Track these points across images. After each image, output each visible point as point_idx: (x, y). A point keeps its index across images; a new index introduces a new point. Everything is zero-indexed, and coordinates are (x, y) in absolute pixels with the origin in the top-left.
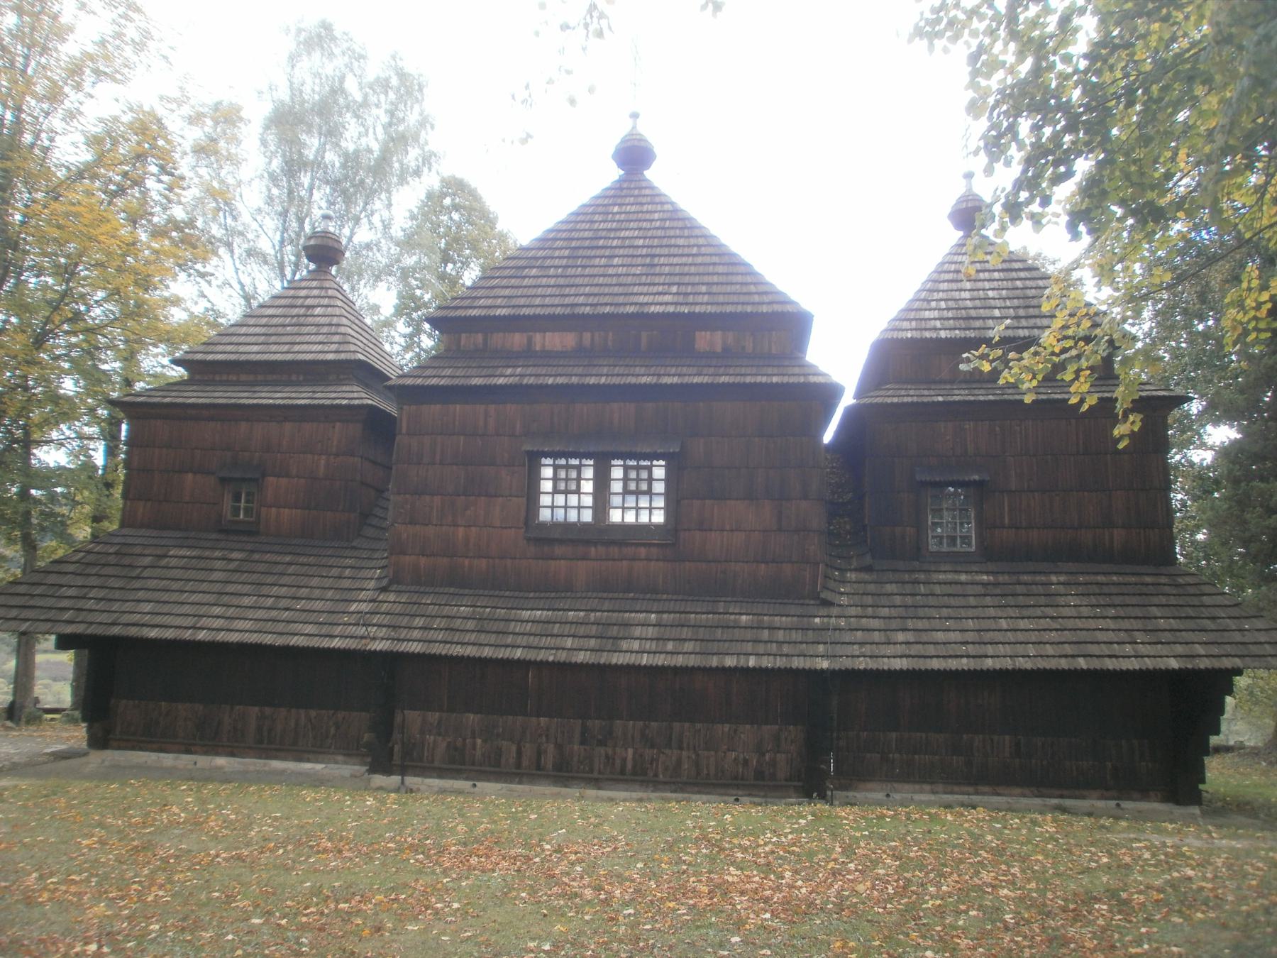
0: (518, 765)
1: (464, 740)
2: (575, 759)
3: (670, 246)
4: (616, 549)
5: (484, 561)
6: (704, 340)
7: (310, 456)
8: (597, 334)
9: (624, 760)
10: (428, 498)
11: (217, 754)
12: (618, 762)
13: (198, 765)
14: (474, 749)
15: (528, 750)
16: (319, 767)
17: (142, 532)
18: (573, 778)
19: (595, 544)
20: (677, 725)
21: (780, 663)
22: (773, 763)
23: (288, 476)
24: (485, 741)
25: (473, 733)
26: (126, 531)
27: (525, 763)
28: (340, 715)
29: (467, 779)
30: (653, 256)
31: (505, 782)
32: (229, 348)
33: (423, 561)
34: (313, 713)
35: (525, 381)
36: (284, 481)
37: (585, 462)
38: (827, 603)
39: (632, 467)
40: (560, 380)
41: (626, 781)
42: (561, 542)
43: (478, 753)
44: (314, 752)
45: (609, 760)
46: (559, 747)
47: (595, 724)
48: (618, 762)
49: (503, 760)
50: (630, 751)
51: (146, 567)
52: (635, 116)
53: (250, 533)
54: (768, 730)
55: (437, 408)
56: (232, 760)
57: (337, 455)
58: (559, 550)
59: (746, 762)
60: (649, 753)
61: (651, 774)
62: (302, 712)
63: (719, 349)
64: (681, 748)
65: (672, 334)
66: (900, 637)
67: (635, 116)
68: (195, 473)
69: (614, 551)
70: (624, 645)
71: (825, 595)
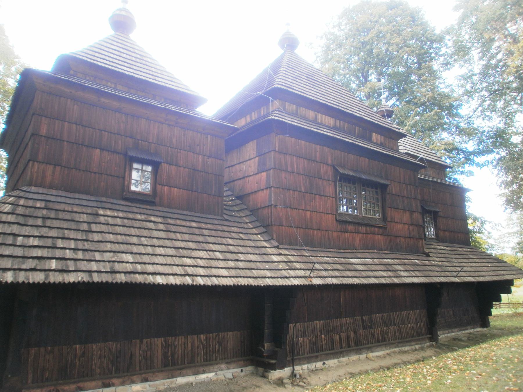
16: (211, 375)
17: (54, 192)
23: (177, 165)
24: (325, 336)
25: (321, 332)
28: (221, 335)
29: (321, 360)
31: (338, 358)
34: (203, 337)
44: (206, 365)
46: (355, 332)
47: (366, 317)
53: (152, 203)
56: (146, 385)
57: (209, 157)
58: (350, 227)
60: (386, 328)
68: (102, 149)
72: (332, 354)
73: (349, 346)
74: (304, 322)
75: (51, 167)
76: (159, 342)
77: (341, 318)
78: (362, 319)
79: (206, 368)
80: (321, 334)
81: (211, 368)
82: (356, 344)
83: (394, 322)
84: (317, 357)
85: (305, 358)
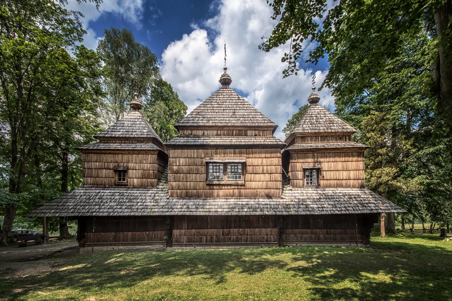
5: (195, 191)
6: (249, 133)
10: (179, 175)
37: (221, 164)
39: (233, 166)
52: (225, 69)
64: (247, 235)
67: (225, 69)
71: (282, 196)
74: (185, 229)
77: (207, 229)
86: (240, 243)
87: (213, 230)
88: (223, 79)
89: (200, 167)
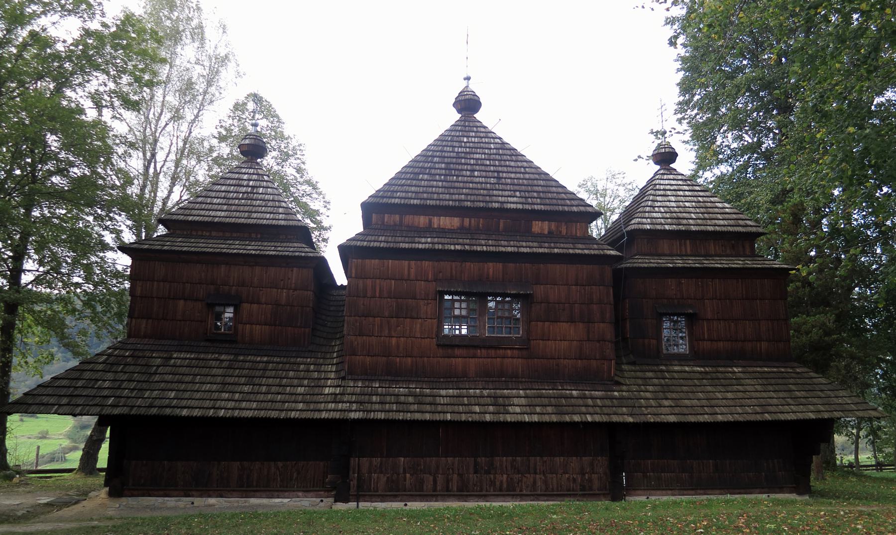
0: (435, 490)
1: (399, 474)
2: (471, 483)
3: (507, 166)
4: (493, 351)
5: (409, 359)
7: (275, 290)
8: (473, 220)
9: (502, 482)
10: (371, 319)
11: (210, 496)
12: (498, 483)
13: (195, 504)
14: (405, 480)
15: (440, 478)
16: (286, 500)
18: (470, 495)
19: (480, 348)
20: (532, 459)
21: (605, 419)
22: (590, 480)
23: (259, 303)
25: (404, 469)
26: (132, 340)
27: (438, 488)
29: (401, 501)
30: (498, 172)
31: (427, 501)
32: (202, 213)
33: (368, 359)
34: (280, 464)
35: (436, 247)
36: (255, 306)
38: (618, 383)
40: (458, 247)
41: (503, 495)
42: (458, 346)
43: (408, 483)
45: (492, 483)
47: (482, 460)
48: (498, 483)
49: (425, 488)
50: (505, 476)
51: (158, 366)
52: (468, 79)
54: (586, 460)
55: (376, 262)
57: (295, 290)
59: (574, 480)
60: (517, 477)
61: (518, 489)
62: (272, 464)
63: (546, 232)
64: (536, 473)
65: (519, 221)
66: (666, 403)
67: (468, 79)
68: (185, 300)
69: (492, 352)
70: (510, 409)
71: (616, 378)
72: (420, 495)
73: (448, 490)
75: (144, 321)
76: (236, 465)
78: (475, 461)
79: (281, 494)
80: (405, 472)
81: (286, 494)
82: (460, 490)
83: (535, 470)
84: (395, 496)
85: (379, 496)
86: (518, 492)
87: (450, 459)
88: (465, 100)
89: (422, 303)
